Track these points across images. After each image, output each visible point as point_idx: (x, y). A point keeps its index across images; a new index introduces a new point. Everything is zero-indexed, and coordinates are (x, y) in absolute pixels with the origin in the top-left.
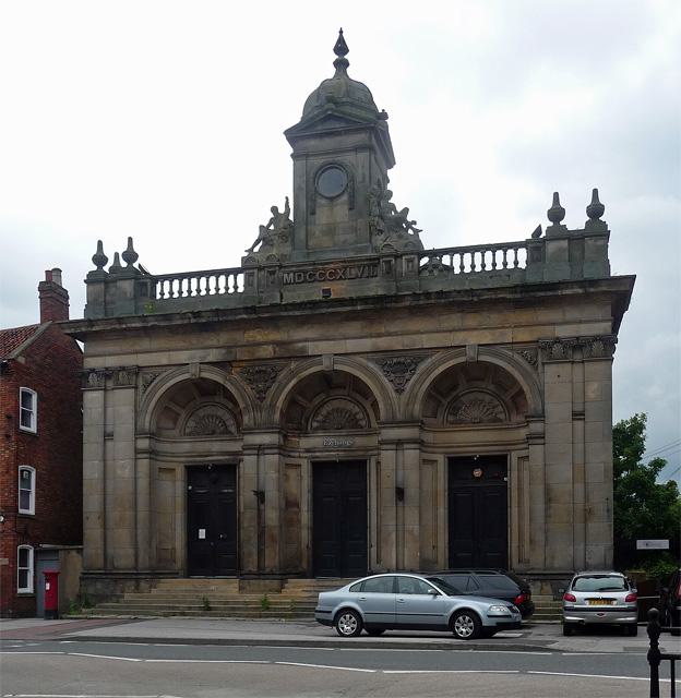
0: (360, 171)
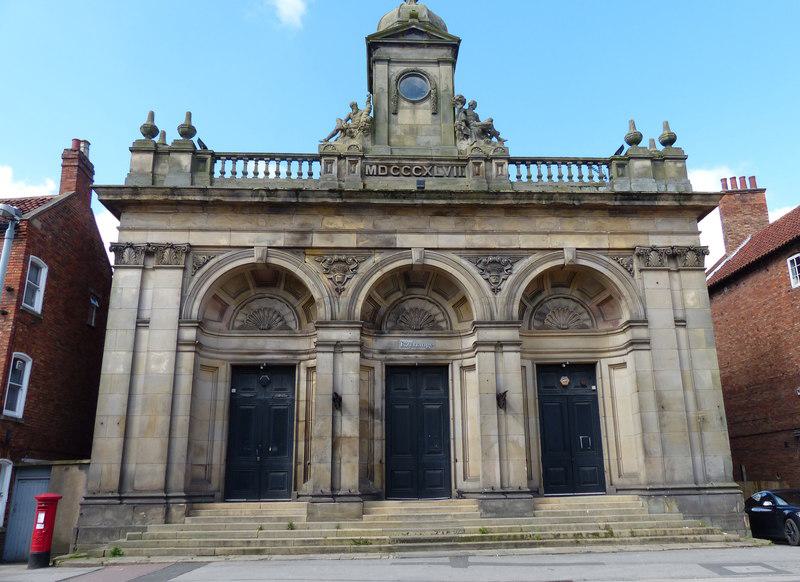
0: (443, 79)
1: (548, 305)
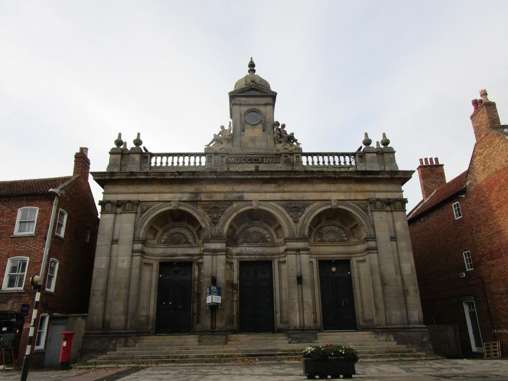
1: (325, 229)
